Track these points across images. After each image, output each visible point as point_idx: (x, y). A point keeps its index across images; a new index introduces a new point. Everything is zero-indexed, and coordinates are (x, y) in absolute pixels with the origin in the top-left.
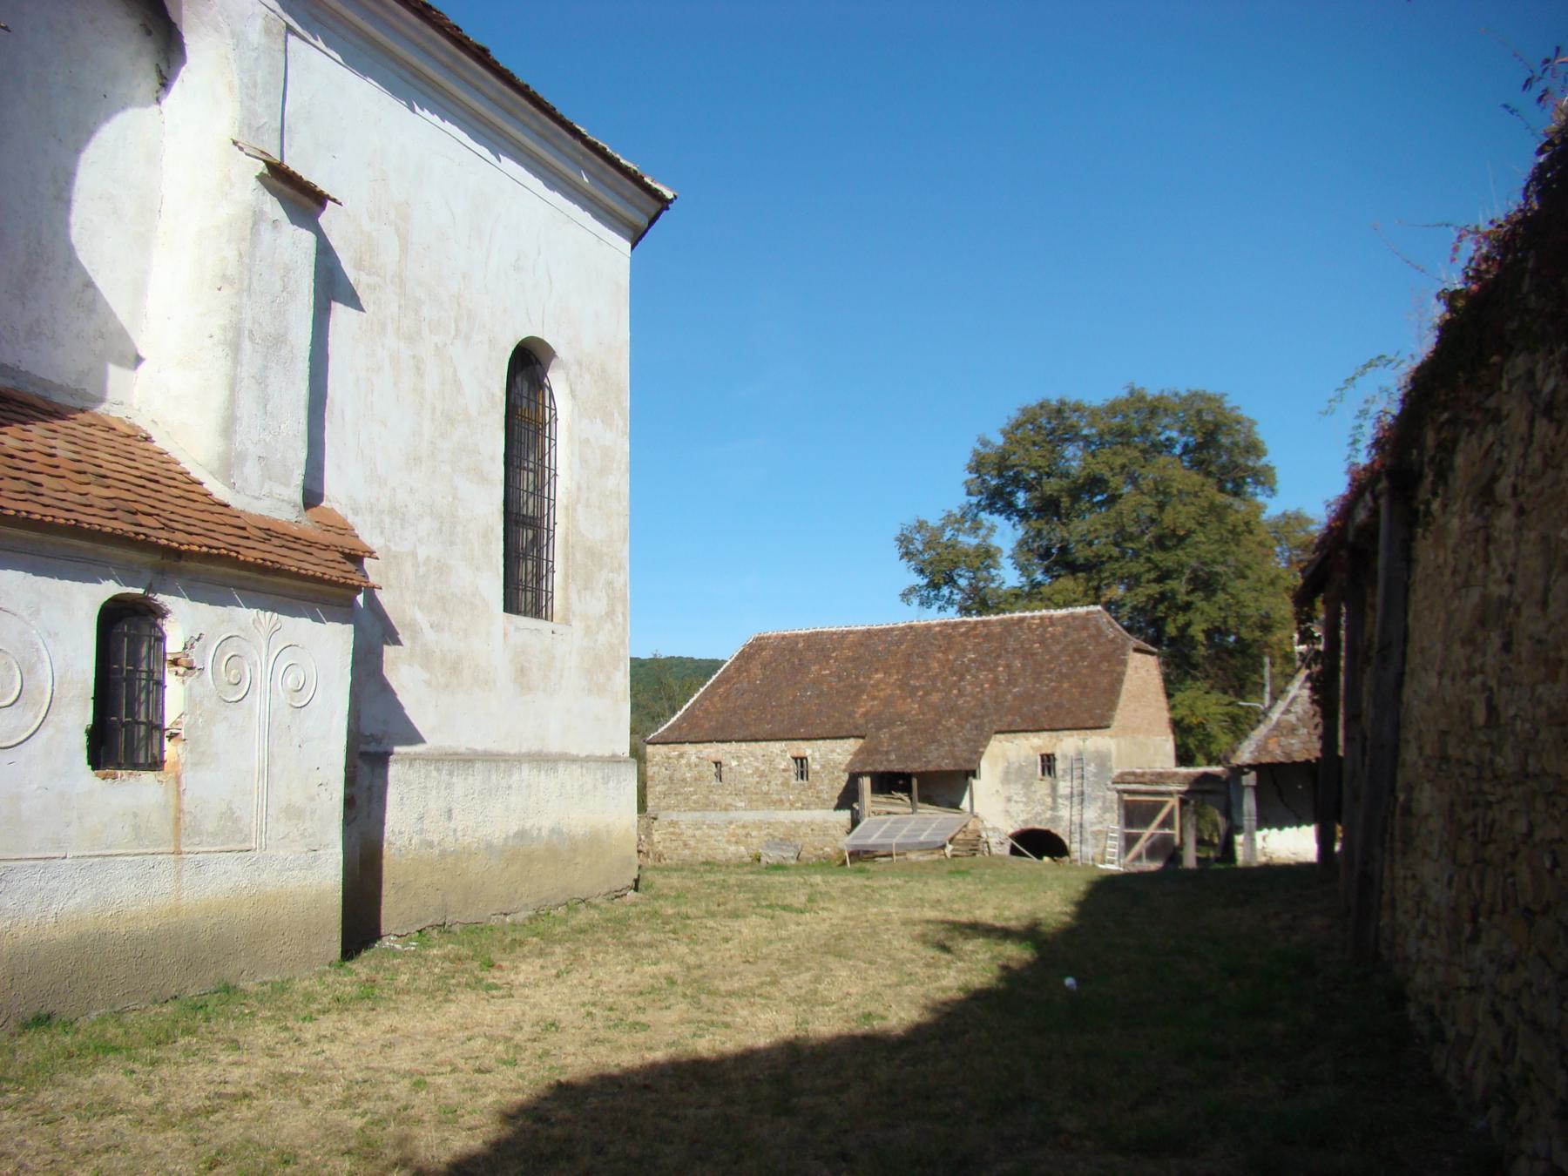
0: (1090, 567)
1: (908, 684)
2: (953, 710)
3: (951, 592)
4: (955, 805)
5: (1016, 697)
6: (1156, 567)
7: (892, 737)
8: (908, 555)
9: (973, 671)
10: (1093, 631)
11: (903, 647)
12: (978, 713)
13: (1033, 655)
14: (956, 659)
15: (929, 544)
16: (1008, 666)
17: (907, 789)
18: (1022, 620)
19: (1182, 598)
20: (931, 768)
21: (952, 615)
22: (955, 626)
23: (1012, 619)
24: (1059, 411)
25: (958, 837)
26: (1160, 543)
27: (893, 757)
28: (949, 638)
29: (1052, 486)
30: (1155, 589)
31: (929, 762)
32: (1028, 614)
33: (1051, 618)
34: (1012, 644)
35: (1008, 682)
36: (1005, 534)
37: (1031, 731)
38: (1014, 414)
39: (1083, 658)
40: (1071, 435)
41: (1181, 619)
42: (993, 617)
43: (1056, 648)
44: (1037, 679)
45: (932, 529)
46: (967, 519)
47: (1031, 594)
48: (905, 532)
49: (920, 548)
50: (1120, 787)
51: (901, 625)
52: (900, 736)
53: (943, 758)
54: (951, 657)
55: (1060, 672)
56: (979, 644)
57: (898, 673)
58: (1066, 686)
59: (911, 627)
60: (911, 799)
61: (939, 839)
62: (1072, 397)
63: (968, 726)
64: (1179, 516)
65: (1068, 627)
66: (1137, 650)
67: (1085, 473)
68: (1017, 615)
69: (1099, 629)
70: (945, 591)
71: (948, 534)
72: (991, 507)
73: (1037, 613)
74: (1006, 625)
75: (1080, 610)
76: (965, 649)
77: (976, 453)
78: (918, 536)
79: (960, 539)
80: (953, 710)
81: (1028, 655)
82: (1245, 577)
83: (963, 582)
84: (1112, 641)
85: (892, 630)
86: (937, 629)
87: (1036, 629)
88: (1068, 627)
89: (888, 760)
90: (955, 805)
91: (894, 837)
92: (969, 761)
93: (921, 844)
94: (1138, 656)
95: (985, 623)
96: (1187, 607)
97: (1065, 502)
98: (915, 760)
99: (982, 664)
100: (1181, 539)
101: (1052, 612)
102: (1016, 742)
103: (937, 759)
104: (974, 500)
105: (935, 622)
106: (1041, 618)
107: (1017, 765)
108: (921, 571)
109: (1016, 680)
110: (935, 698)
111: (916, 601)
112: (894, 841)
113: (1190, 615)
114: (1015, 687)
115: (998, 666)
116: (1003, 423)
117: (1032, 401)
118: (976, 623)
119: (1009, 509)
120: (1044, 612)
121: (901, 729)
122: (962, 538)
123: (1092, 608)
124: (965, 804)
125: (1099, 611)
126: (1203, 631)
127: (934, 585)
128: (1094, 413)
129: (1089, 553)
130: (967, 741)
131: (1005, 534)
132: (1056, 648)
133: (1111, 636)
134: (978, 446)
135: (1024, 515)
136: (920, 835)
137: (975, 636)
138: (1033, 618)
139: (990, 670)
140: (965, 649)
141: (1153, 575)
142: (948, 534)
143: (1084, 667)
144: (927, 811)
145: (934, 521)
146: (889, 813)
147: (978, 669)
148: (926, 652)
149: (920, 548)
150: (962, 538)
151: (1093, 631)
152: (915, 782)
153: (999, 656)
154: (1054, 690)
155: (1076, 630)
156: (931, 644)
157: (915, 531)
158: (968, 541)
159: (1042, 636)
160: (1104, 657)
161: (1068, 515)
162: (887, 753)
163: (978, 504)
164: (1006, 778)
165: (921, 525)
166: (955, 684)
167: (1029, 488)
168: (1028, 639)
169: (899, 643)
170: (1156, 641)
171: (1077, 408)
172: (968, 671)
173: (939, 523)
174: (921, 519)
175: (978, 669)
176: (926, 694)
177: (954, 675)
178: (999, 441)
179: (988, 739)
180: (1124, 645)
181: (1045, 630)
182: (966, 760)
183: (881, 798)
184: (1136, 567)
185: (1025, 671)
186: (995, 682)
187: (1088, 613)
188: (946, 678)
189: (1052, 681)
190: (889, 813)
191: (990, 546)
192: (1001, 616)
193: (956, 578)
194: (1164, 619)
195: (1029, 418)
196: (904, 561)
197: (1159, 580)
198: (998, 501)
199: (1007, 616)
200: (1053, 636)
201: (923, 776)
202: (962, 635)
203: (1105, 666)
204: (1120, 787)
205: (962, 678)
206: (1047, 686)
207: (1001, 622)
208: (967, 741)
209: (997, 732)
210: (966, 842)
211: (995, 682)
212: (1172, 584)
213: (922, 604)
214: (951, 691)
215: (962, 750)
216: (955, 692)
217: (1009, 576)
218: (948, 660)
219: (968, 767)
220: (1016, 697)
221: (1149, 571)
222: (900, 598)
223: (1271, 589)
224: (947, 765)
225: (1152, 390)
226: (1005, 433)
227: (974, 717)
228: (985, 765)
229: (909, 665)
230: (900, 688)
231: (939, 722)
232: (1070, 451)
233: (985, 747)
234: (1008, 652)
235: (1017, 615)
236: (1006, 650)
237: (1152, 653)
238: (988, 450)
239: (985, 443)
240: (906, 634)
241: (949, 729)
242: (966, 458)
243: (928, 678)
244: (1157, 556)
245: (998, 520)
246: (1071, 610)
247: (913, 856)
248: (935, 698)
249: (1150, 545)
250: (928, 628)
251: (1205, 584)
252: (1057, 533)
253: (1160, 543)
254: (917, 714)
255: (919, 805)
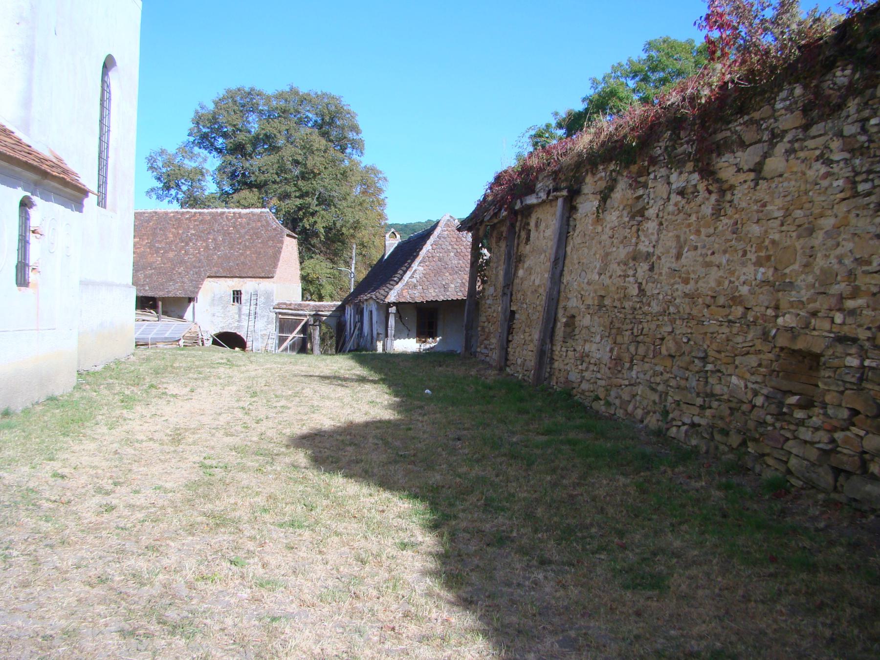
0: (260, 186)
1: (154, 246)
2: (182, 262)
3: (177, 193)
4: (181, 317)
5: (219, 257)
6: (300, 190)
7: (146, 276)
8: (152, 168)
9: (194, 241)
10: (264, 223)
11: (151, 224)
12: (197, 265)
13: (229, 234)
14: (183, 233)
15: (166, 164)
16: (214, 239)
17: (154, 307)
18: (223, 213)
19: (313, 208)
20: (170, 295)
21: (175, 207)
22: (183, 214)
23: (217, 212)
24: (249, 93)
25: (187, 335)
26: (303, 176)
27: (147, 288)
28: (179, 220)
29: (241, 137)
30: (298, 202)
31: (169, 292)
32: (226, 210)
33: (240, 214)
34: (216, 227)
35: (215, 248)
36: (212, 162)
37: (228, 277)
38: (222, 93)
39: (258, 238)
40: (254, 109)
41: (312, 220)
42: (205, 211)
43: (243, 231)
44: (231, 248)
45: (169, 155)
46: (185, 150)
47: (225, 198)
48: (152, 155)
49: (161, 165)
50: (278, 311)
51: (149, 211)
52: (150, 276)
53: (178, 290)
54: (180, 232)
55: (245, 245)
56: (197, 225)
57: (148, 239)
58: (248, 253)
59: (156, 213)
60: (157, 313)
61: (177, 336)
62: (258, 87)
63: (192, 272)
64: (314, 162)
65: (250, 219)
66: (288, 235)
67: (264, 132)
68: (220, 210)
69: (267, 222)
70: (173, 192)
71: (178, 159)
72: (200, 145)
73: (232, 210)
74: (214, 216)
75: (258, 211)
76: (189, 228)
77: (197, 112)
78: (159, 158)
79: (185, 162)
80: (182, 262)
81: (227, 233)
82: (345, 199)
83: (184, 188)
84: (275, 229)
85: (144, 213)
86: (172, 215)
87: (231, 219)
88: (250, 219)
89: (144, 289)
90: (181, 317)
91: (149, 334)
92: (193, 292)
93: (166, 338)
94: (288, 238)
95: (200, 213)
96: (313, 214)
97: (249, 148)
98: (161, 290)
99: (199, 237)
100: (315, 175)
101: (240, 210)
102: (219, 282)
103: (174, 290)
104: (192, 139)
105: (170, 211)
106: (234, 213)
107: (219, 296)
108: (159, 179)
109: (219, 248)
110: (171, 255)
111: (155, 197)
112: (150, 336)
113: (315, 218)
114: (218, 252)
115: (209, 239)
116: (214, 97)
117: (233, 87)
118: (195, 213)
119: (212, 147)
120: (236, 210)
121: (150, 272)
122: (186, 162)
123: (263, 210)
124: (188, 315)
125: (268, 212)
126: (323, 227)
127: (167, 187)
128: (268, 98)
129: (262, 178)
130: (192, 281)
131: (212, 162)
132: (243, 231)
133: (274, 226)
134: (199, 109)
135: (220, 151)
136: (165, 334)
137: (195, 221)
138: (229, 213)
139: (204, 241)
140: (189, 228)
141: (298, 194)
142: (178, 159)
143: (259, 243)
144: (166, 320)
145: (172, 149)
146: (144, 320)
147: (197, 240)
148: (165, 228)
149: (161, 165)
150: (186, 162)
151: (264, 223)
152: (160, 303)
153: (209, 233)
154: (242, 254)
155: (254, 221)
156: (168, 223)
157: (158, 155)
158: (189, 164)
159: (235, 223)
160: (270, 238)
161: (250, 155)
162: (143, 285)
163: (193, 143)
164: (213, 302)
165: (162, 152)
166: (183, 248)
167: (225, 135)
168: (227, 225)
169: (148, 221)
170: (293, 230)
171: (259, 94)
172: (190, 240)
173: (174, 152)
174: (163, 148)
175: (197, 240)
176: (166, 252)
177: (182, 242)
178: (211, 107)
179: (203, 280)
180: (282, 231)
181: (236, 220)
182: (191, 292)
183: (139, 312)
184: (290, 189)
185: (225, 243)
186: (207, 248)
187: (261, 212)
188: (178, 244)
189: (240, 249)
190: (144, 320)
191: (203, 168)
192: (210, 210)
193: (180, 184)
194: (301, 220)
195: (231, 95)
196: (150, 172)
197: (300, 197)
198: (205, 140)
199: (214, 210)
200: (241, 224)
201: (164, 299)
202: (187, 219)
203: (270, 243)
204: (278, 311)
205: (187, 244)
206: (237, 252)
207: (210, 214)
208: (192, 281)
209: (209, 277)
210: (191, 338)
211: (207, 248)
212: (308, 200)
213: (158, 198)
214: (180, 251)
215: (188, 286)
216: (183, 252)
217: (211, 187)
218: (178, 233)
219: (192, 296)
220: (219, 257)
221: (295, 191)
222: (145, 194)
223: (360, 207)
224: (180, 294)
225: (303, 90)
226: (216, 103)
227: (195, 267)
228: (201, 296)
229: (154, 235)
230: (150, 248)
231: (173, 269)
232: (253, 117)
233: (202, 284)
234: (214, 231)
235: (220, 210)
236: (213, 230)
237: (295, 238)
238: (204, 112)
239: (202, 108)
240: (153, 216)
241: (180, 274)
242: (192, 115)
243: (166, 243)
244: (300, 183)
245: (204, 152)
246: (251, 210)
247: (161, 345)
248: (171, 255)
249: (297, 176)
250: (167, 214)
251: (325, 201)
252: (239, 163)
253: (303, 176)
254: (160, 264)
255: (162, 316)
